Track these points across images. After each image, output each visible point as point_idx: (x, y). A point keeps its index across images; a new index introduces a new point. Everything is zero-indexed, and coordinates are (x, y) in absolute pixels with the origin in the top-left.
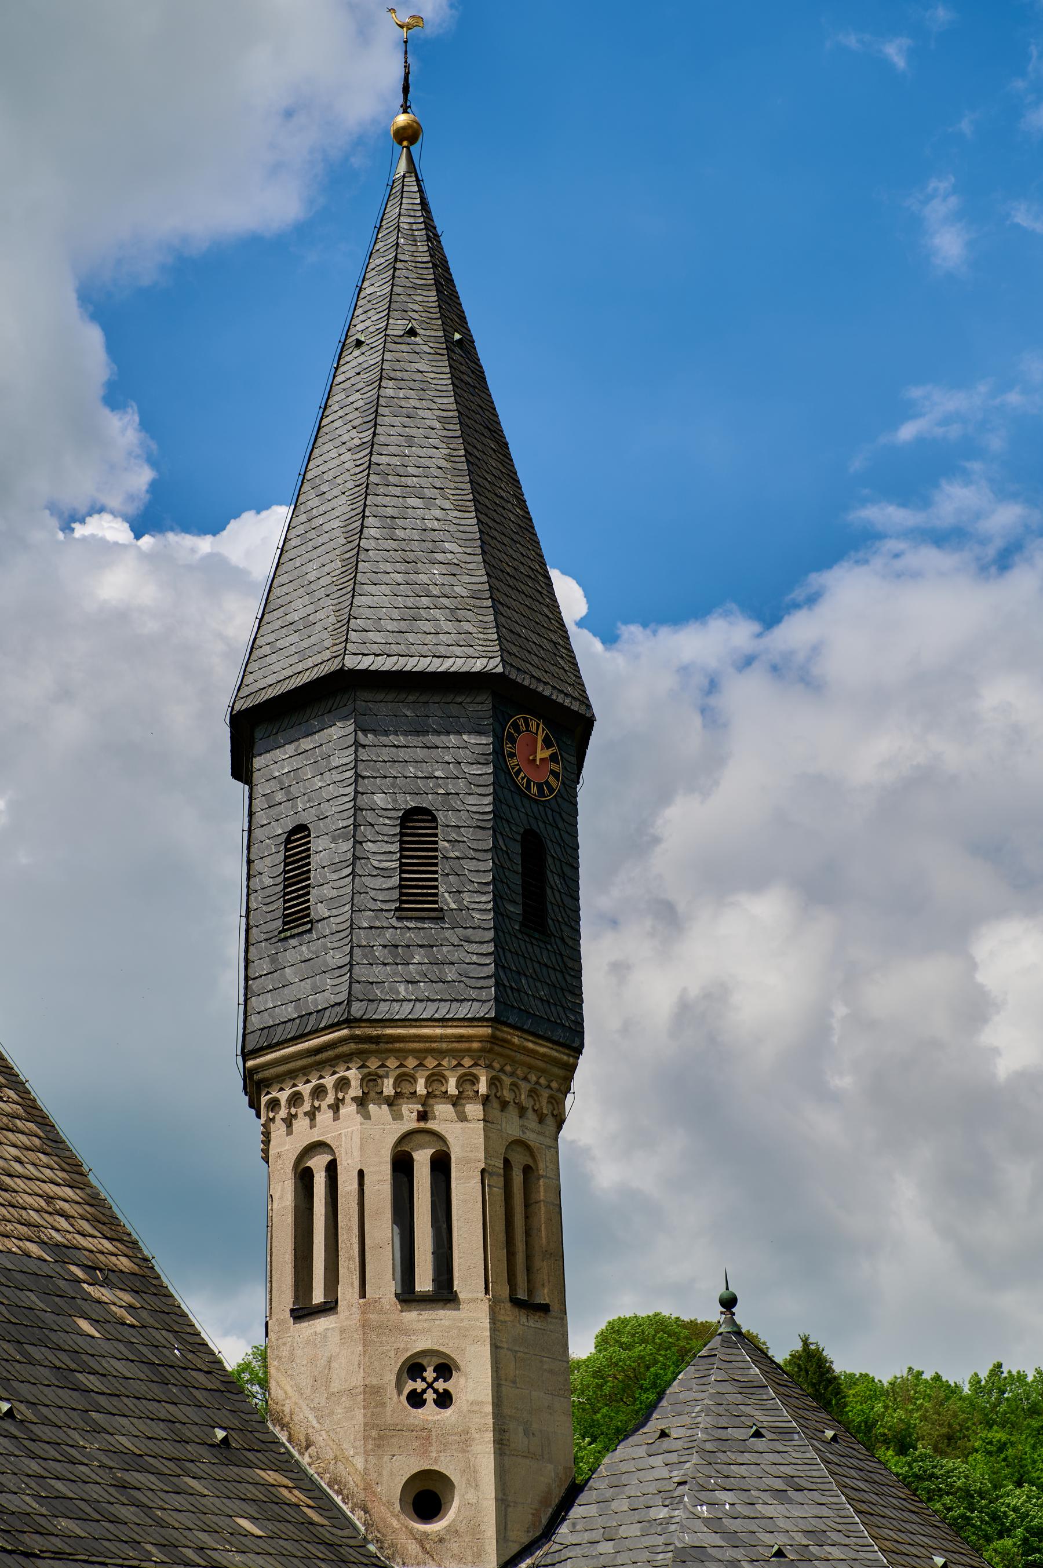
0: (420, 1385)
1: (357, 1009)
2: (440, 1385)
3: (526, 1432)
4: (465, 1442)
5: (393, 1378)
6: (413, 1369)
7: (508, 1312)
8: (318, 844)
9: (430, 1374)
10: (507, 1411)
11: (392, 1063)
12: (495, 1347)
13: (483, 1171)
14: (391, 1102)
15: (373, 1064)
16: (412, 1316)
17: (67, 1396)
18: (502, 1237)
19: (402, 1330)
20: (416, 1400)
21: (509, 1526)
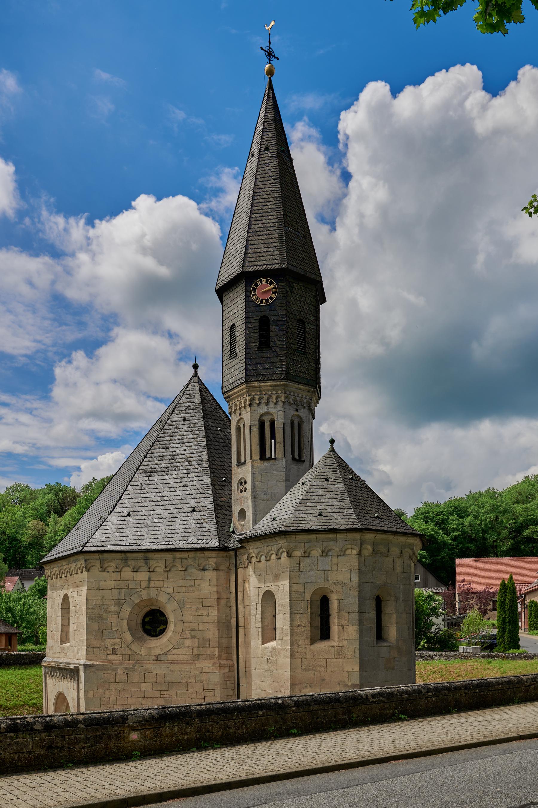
2: (245, 486)
3: (265, 494)
5: (236, 487)
10: (257, 489)
13: (250, 426)
21: (257, 519)
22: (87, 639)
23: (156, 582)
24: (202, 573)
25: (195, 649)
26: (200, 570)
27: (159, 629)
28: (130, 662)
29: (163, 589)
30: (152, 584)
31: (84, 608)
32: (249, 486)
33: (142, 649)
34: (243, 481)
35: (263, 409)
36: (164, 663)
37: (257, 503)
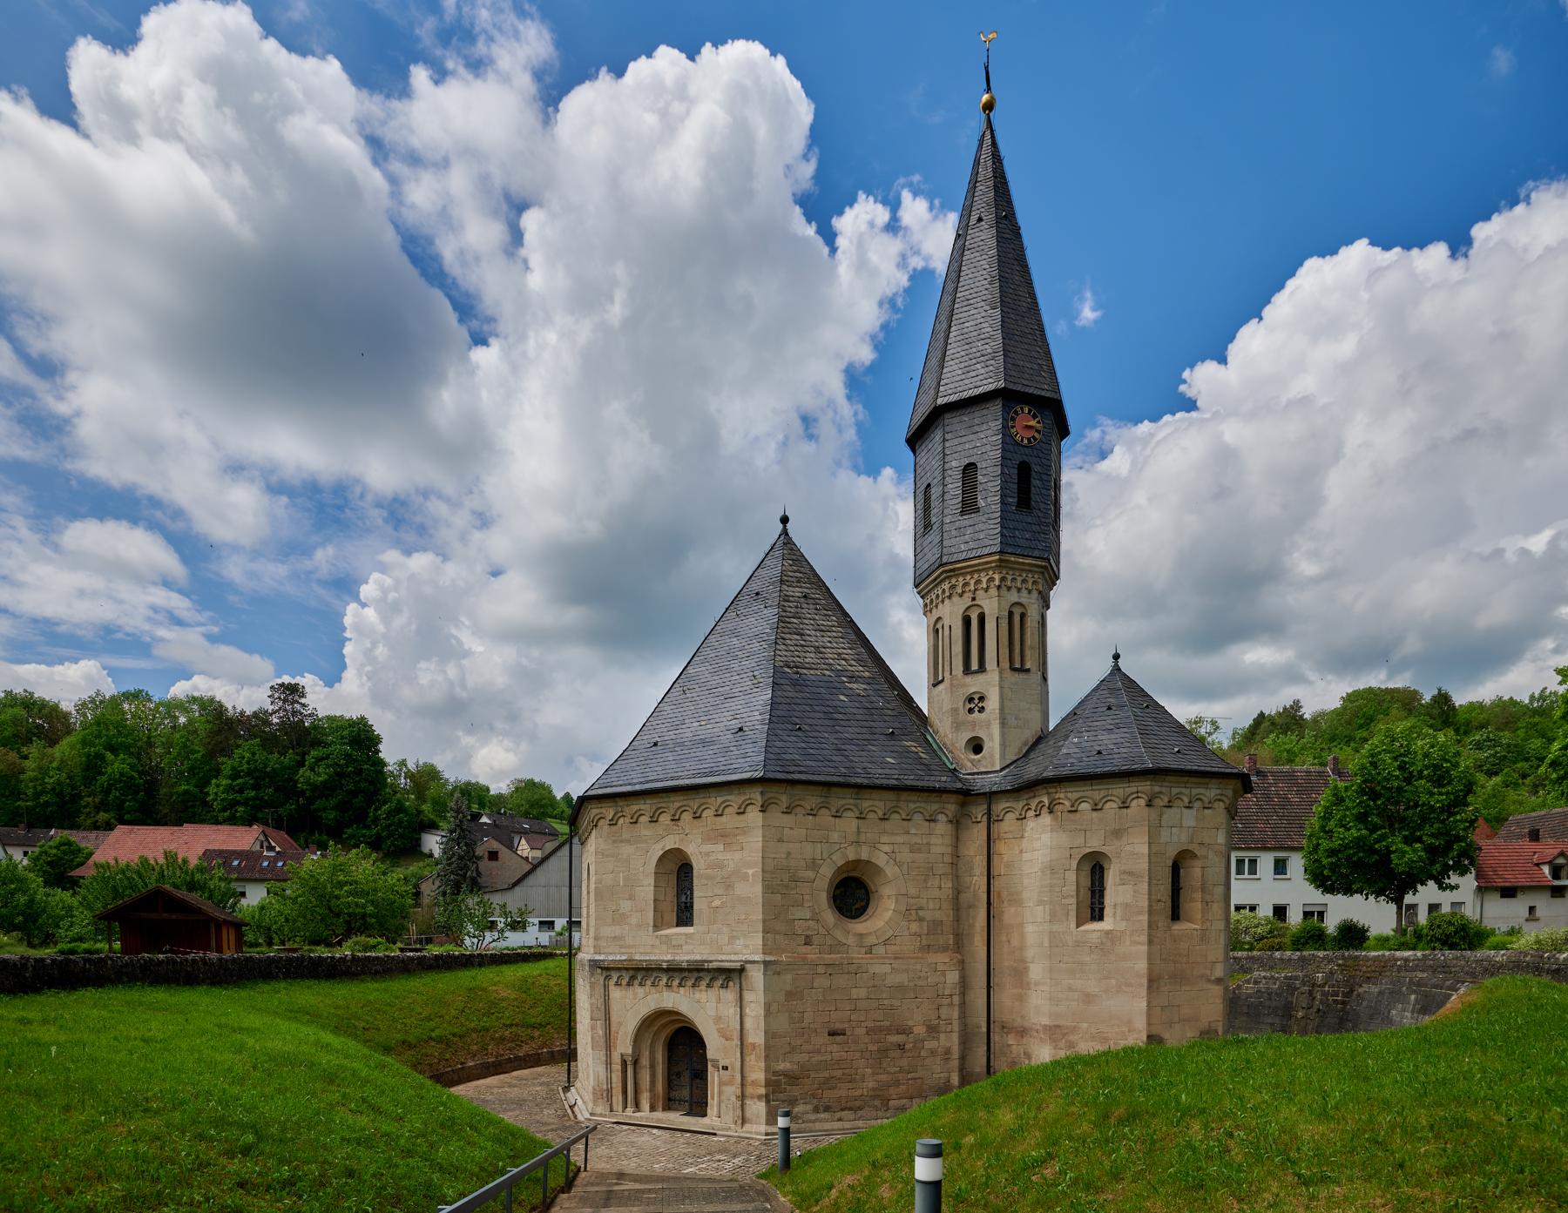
0: (973, 706)
1: (945, 560)
2: (980, 705)
3: (1016, 719)
4: (988, 724)
5: (962, 704)
6: (971, 700)
7: (1008, 673)
8: (933, 490)
9: (976, 701)
11: (961, 579)
12: (1001, 687)
14: (961, 595)
15: (953, 581)
16: (969, 679)
17: (827, 722)
18: (1007, 643)
19: (964, 685)
20: (971, 711)
22: (764, 921)
23: (868, 835)
24: (932, 824)
25: (924, 937)
26: (929, 821)
27: (856, 906)
28: (832, 956)
29: (877, 846)
30: (862, 839)
31: (754, 871)
32: (993, 703)
33: (850, 937)
34: (976, 697)
35: (1013, 597)
36: (884, 958)
37: (1006, 730)
